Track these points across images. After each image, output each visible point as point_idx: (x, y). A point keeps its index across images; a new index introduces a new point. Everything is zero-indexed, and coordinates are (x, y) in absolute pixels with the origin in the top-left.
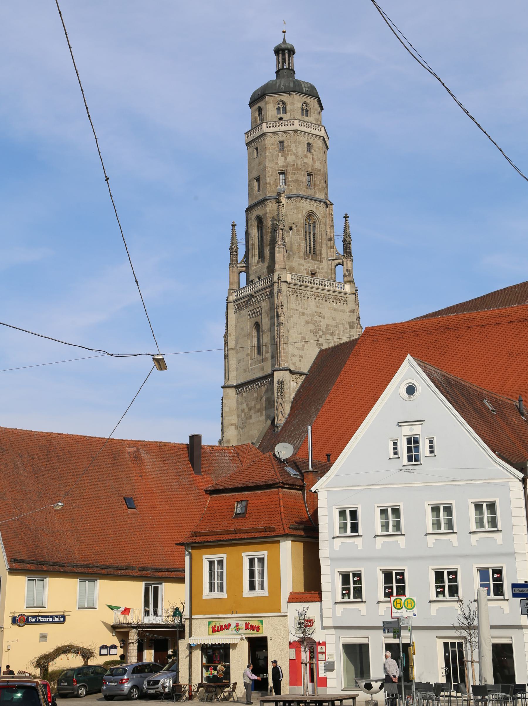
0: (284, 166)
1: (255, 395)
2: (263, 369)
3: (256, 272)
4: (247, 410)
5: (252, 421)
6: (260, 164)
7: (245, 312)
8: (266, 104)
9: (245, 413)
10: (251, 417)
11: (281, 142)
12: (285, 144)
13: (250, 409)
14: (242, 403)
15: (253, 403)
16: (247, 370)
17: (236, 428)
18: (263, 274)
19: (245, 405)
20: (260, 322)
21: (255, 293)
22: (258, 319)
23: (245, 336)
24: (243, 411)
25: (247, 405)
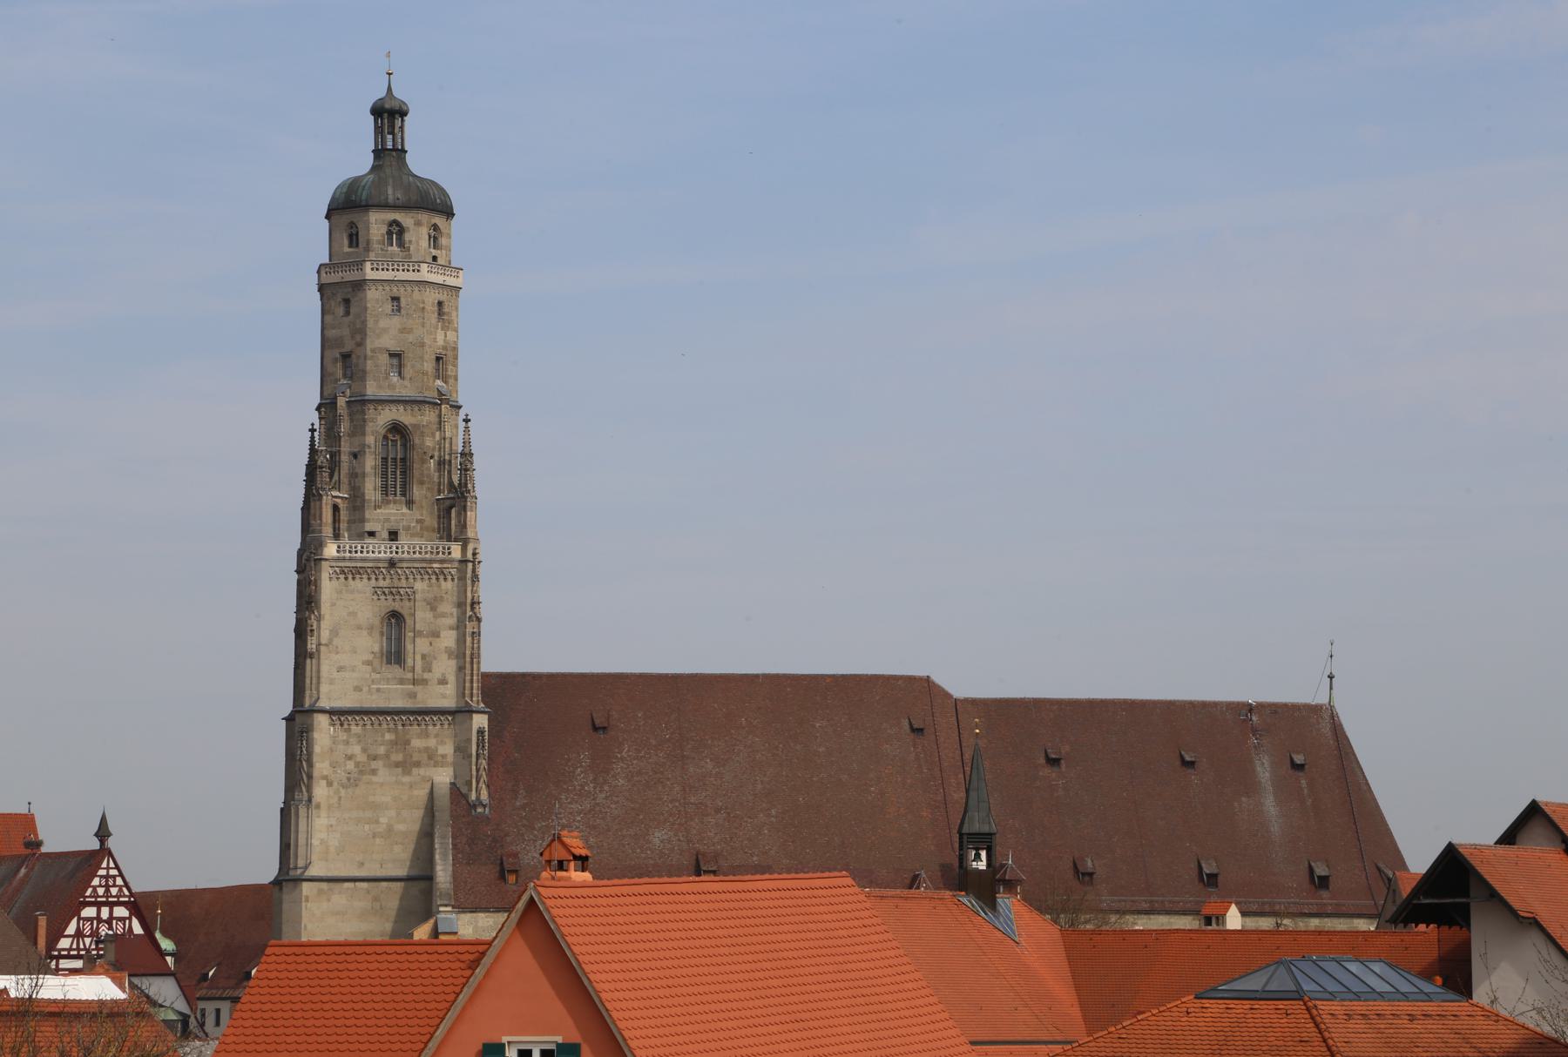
0: (445, 348)
1: (388, 736)
2: (413, 695)
3: (387, 520)
4: (362, 758)
5: (375, 779)
6: (403, 330)
7: (362, 585)
8: (418, 224)
9: (357, 764)
10: (374, 772)
11: (440, 304)
12: (446, 310)
13: (375, 758)
14: (347, 743)
15: (382, 750)
16: (365, 689)
17: (330, 784)
18: (407, 528)
19: (357, 749)
20: (405, 612)
21: (401, 560)
22: (397, 606)
23: (359, 627)
24: (350, 758)
25: (364, 750)
